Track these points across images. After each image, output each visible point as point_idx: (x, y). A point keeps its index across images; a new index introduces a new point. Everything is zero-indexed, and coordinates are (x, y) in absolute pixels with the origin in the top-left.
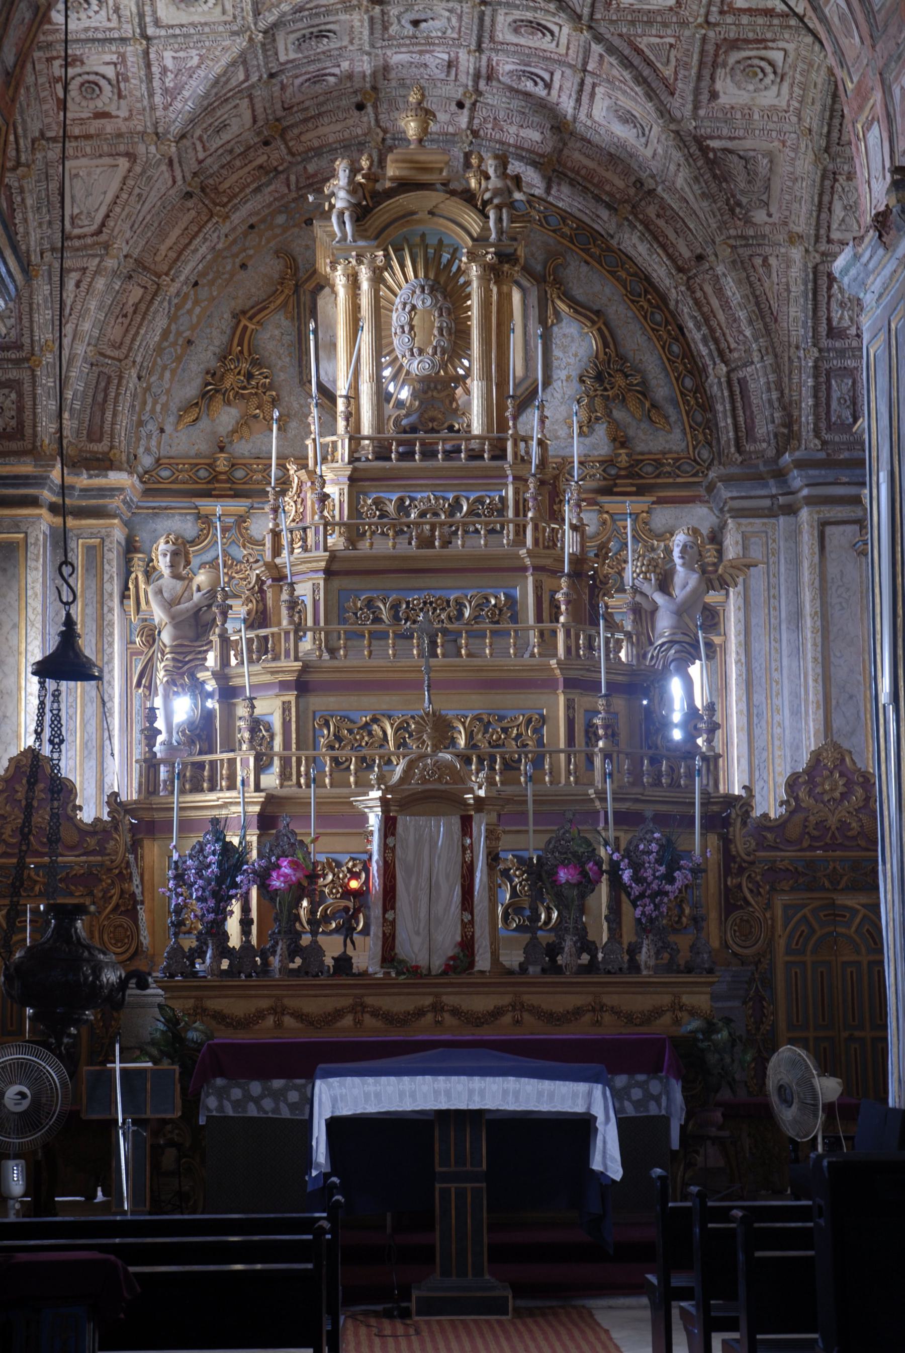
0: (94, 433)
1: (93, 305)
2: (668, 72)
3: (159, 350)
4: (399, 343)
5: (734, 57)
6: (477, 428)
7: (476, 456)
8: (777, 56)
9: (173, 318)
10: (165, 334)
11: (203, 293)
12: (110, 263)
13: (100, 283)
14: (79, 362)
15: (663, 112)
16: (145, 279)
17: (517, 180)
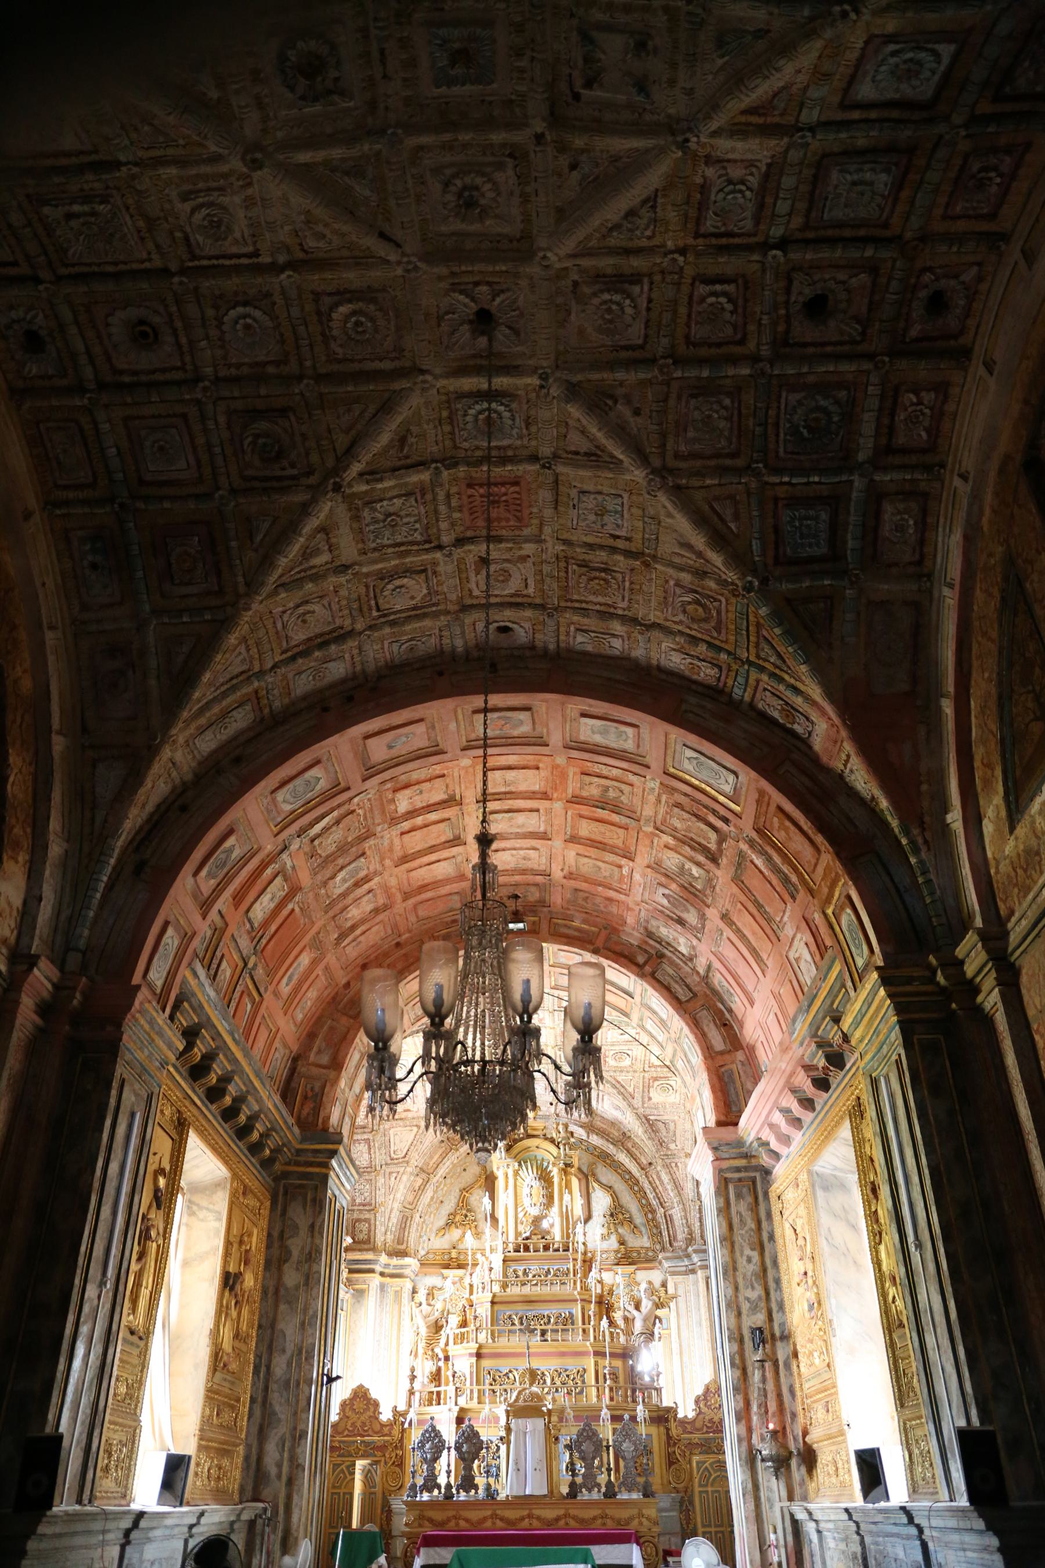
0: (400, 1241)
1: (401, 1187)
2: (631, 1090)
3: (429, 1205)
4: (526, 1202)
5: (657, 1083)
6: (558, 1238)
7: (557, 1250)
8: (672, 1083)
9: (435, 1192)
10: (432, 1198)
11: (448, 1181)
12: (409, 1169)
13: (405, 1178)
14: (395, 1211)
15: (630, 1105)
16: (424, 1176)
17: (572, 1133)
